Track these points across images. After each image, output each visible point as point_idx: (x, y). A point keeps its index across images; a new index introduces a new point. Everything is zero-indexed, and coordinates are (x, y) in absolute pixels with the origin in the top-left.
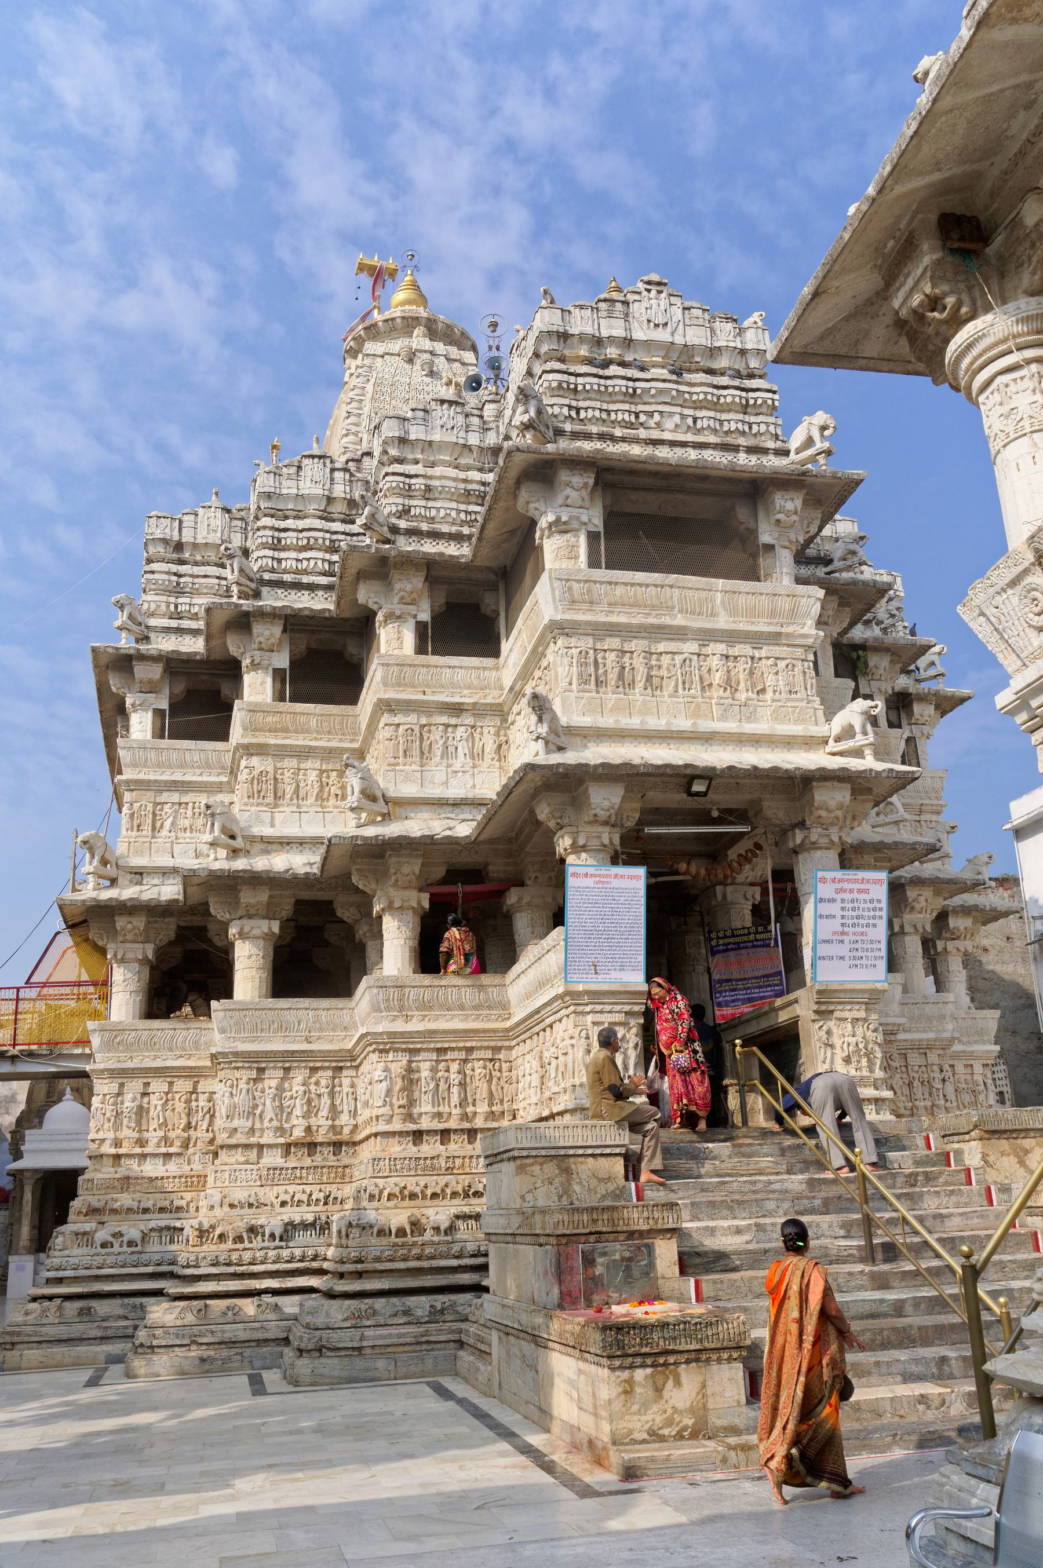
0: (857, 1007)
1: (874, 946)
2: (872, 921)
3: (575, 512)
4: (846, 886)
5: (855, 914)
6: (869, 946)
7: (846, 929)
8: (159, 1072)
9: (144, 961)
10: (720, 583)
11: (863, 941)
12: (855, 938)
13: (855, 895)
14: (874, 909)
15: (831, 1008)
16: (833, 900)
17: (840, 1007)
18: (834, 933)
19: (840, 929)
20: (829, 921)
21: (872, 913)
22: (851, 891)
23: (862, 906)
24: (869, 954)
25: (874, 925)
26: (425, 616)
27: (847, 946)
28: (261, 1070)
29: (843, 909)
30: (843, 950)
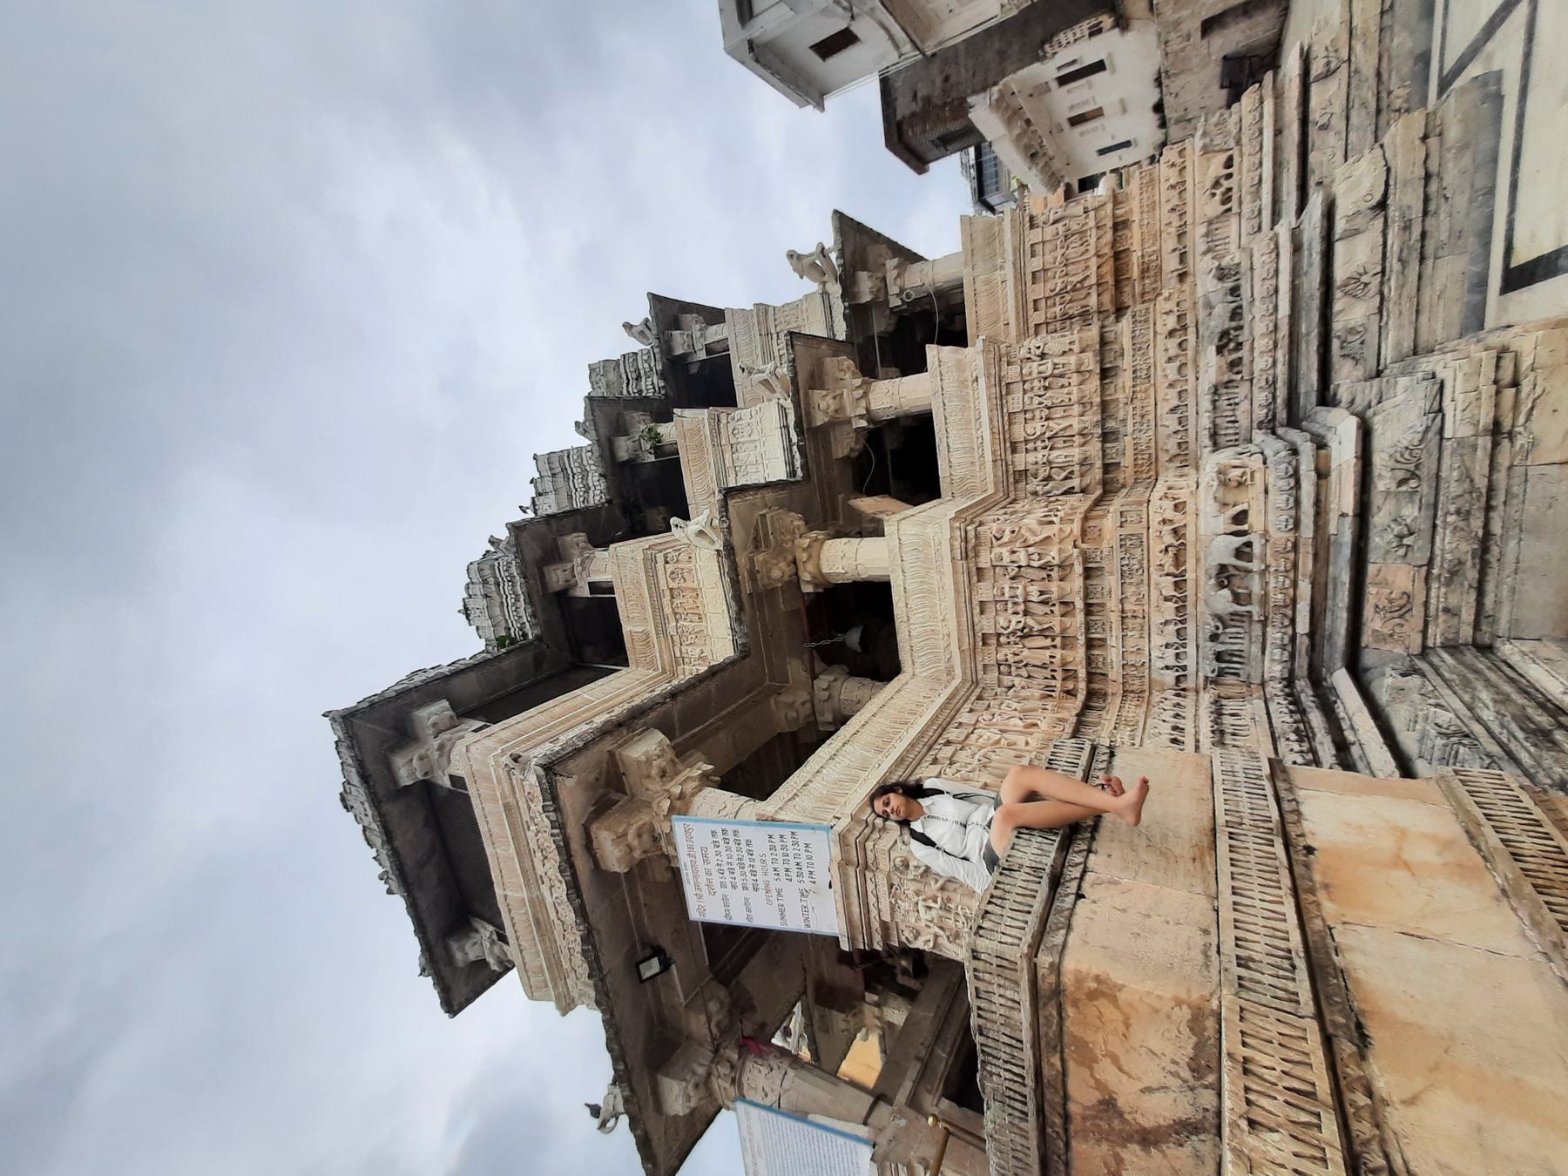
0: (870, 886)
1: (778, 845)
2: (744, 848)
4: (703, 880)
5: (738, 871)
6: (780, 852)
7: (761, 886)
10: (489, 850)
11: (774, 861)
12: (771, 871)
13: (713, 867)
14: (726, 841)
15: (876, 925)
16: (725, 898)
17: (874, 912)
18: (769, 902)
19: (762, 892)
20: (752, 907)
21: (732, 844)
22: (708, 873)
23: (724, 858)
24: (791, 853)
25: (748, 843)
27: (783, 884)
29: (734, 887)
30: (791, 891)
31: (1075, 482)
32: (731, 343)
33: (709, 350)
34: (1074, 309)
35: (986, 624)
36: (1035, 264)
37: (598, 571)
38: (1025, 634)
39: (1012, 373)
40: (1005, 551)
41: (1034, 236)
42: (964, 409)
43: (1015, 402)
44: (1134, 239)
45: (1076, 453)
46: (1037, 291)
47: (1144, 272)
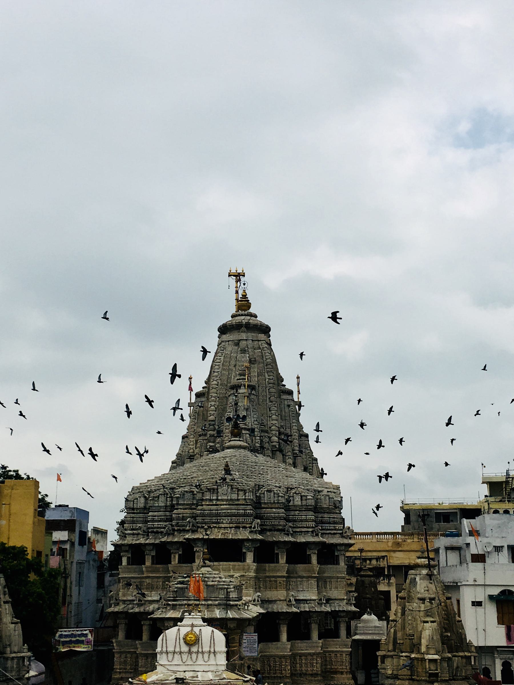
3: (200, 548)
8: (129, 652)
9: (126, 624)
10: (231, 563)
26: (180, 553)
28: (147, 657)
31: (292, 668)
32: (337, 566)
33: (338, 556)
34: (328, 663)
35: (272, 659)
36: (338, 655)
37: (281, 555)
38: (270, 666)
39: (315, 657)
40: (284, 664)
41: (344, 655)
42: (310, 647)
43: (309, 658)
44: (339, 676)
45: (298, 669)
46: (333, 655)
47: (332, 677)
